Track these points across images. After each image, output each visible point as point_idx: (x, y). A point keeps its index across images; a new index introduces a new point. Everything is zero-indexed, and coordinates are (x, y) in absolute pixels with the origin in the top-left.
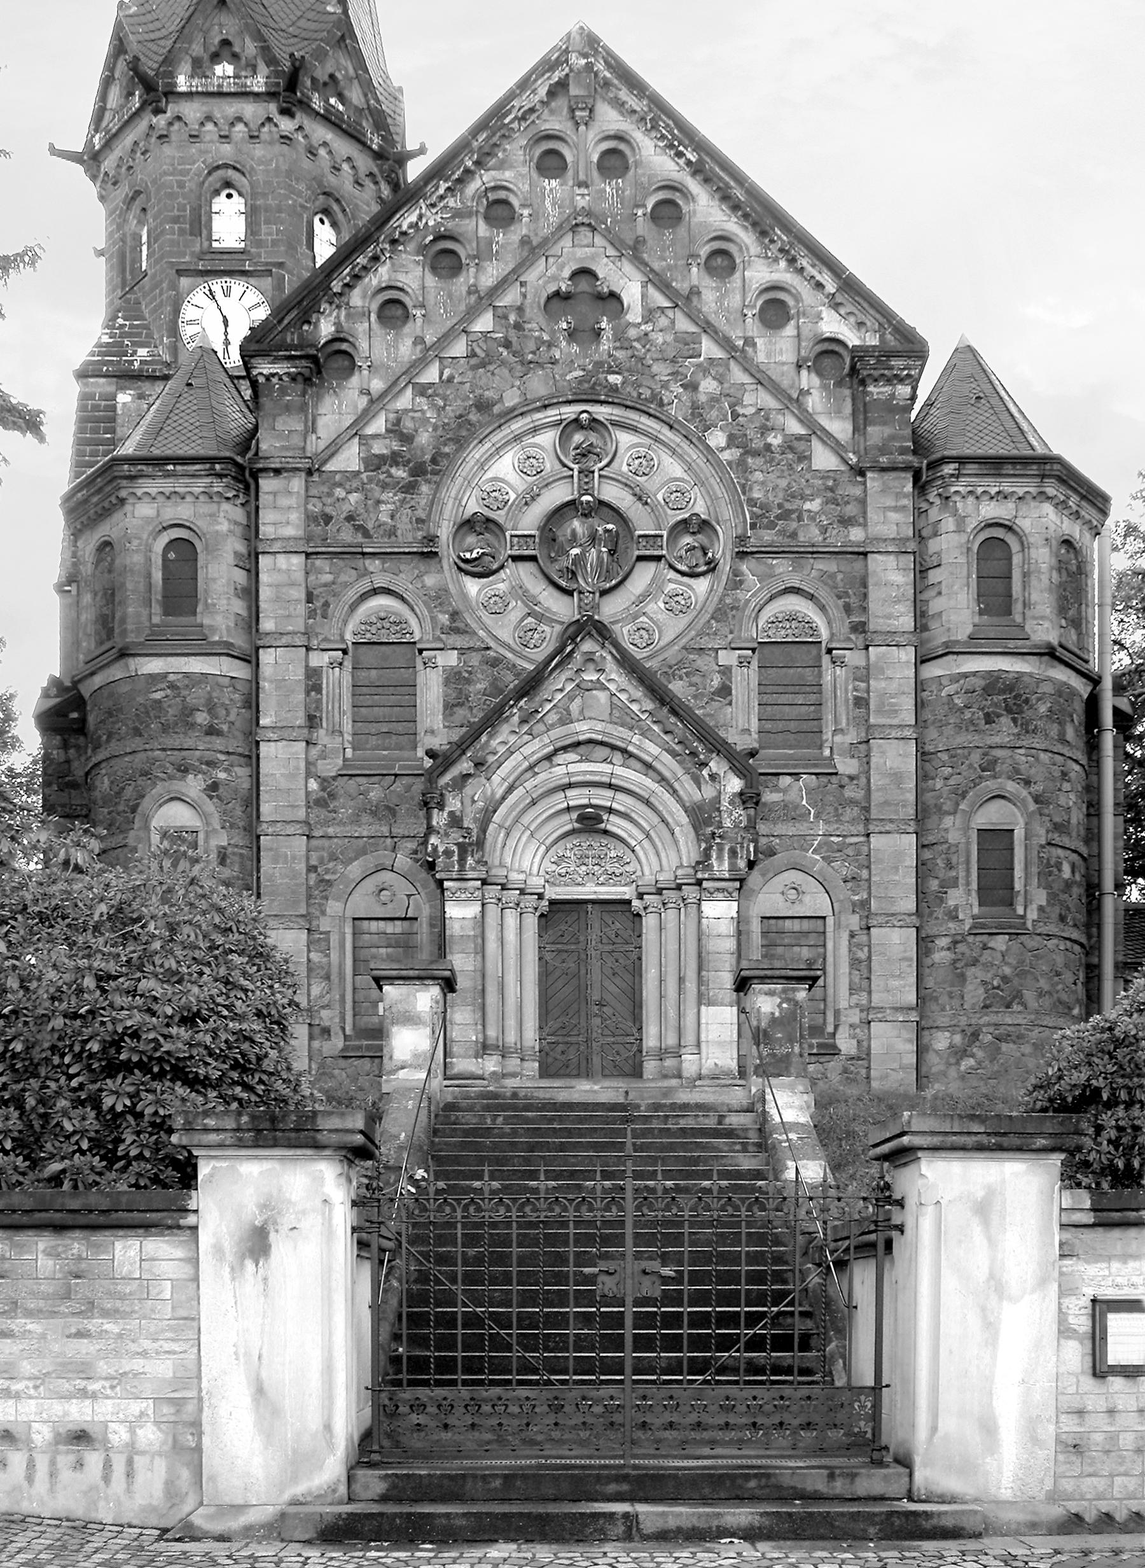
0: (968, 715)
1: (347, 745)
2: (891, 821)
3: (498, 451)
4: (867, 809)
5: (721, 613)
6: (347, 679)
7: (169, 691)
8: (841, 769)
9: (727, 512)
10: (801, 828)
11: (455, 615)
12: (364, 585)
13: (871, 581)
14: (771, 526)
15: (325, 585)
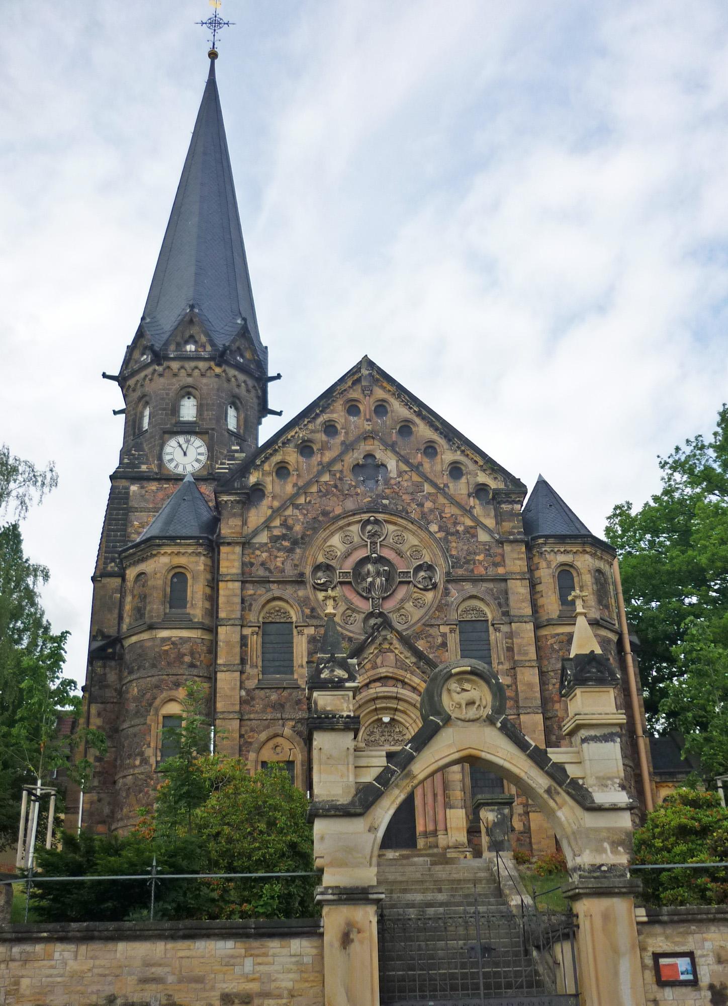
2: (530, 707)
3: (332, 534)
4: (517, 701)
5: (440, 608)
6: (260, 640)
7: (172, 646)
9: (441, 561)
11: (313, 610)
12: (269, 595)
13: (510, 592)
14: (461, 567)
15: (251, 595)
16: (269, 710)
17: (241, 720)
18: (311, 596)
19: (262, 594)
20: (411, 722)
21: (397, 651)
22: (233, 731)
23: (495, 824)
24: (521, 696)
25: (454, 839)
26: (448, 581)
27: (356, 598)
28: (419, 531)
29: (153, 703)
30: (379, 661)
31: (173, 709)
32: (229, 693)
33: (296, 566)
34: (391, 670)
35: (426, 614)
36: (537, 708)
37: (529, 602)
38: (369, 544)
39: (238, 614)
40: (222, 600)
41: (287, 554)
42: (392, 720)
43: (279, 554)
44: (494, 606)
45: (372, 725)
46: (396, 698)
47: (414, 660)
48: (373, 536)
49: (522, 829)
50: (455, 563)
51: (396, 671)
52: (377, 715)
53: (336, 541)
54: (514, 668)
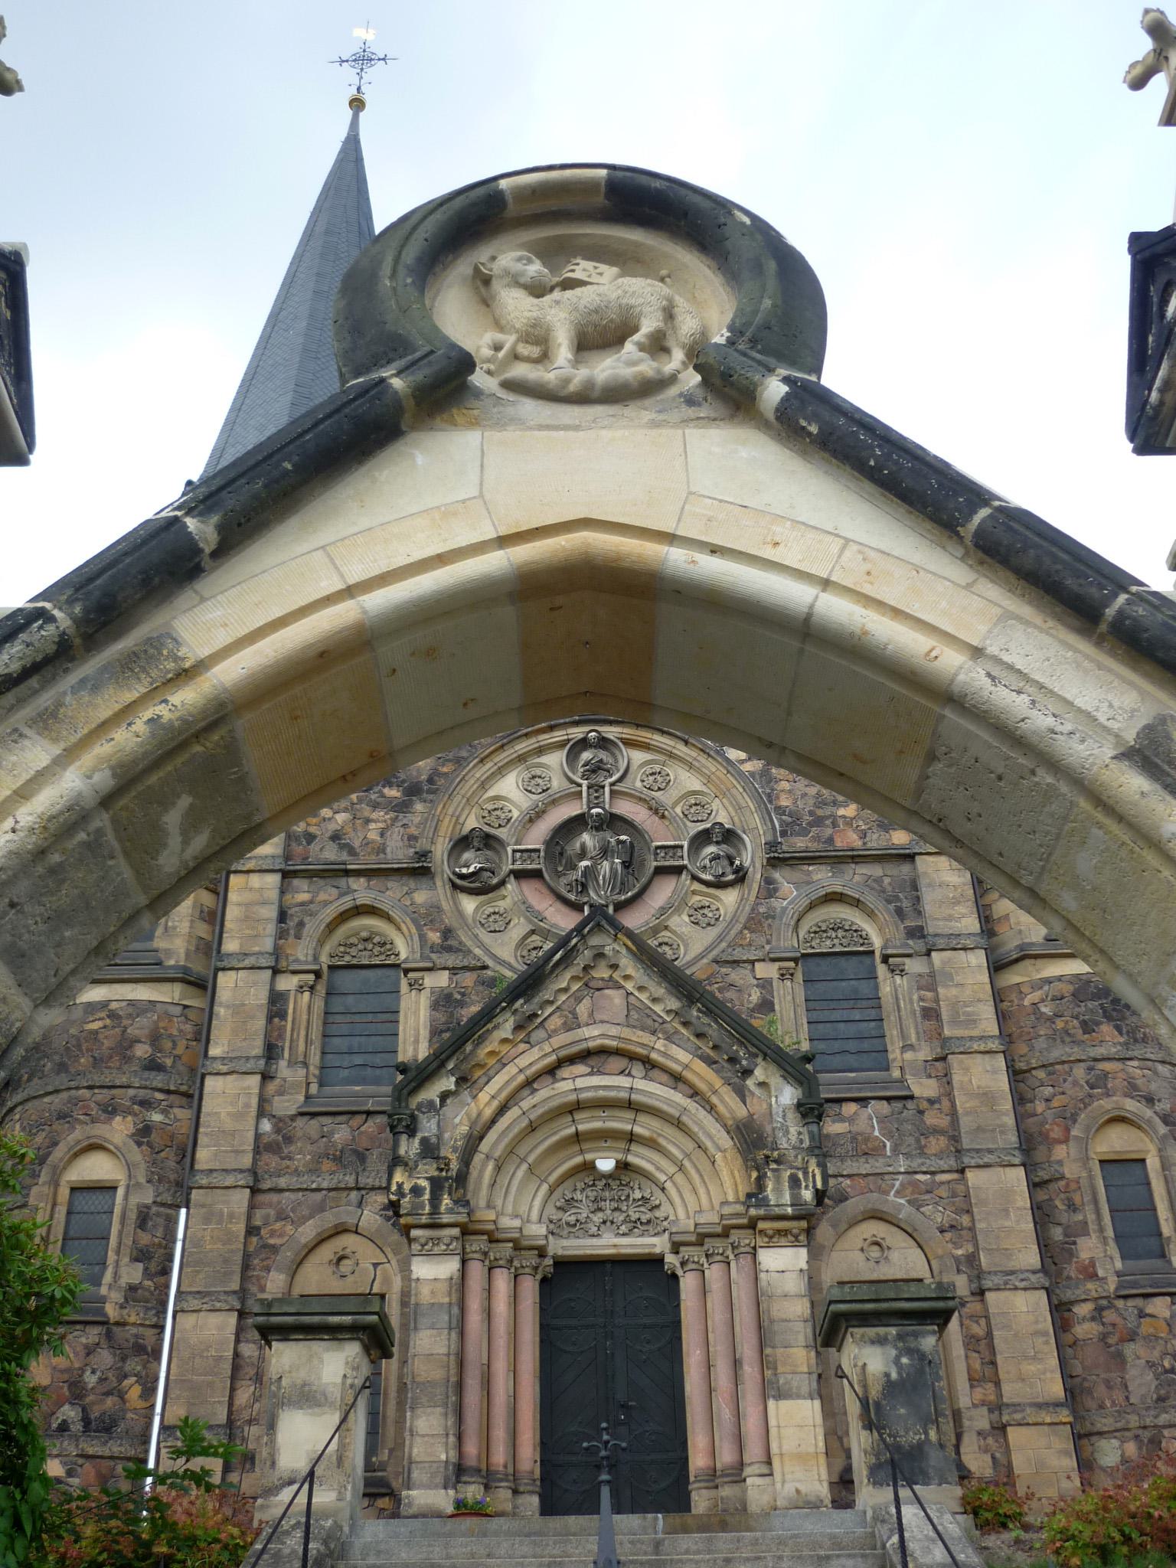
0: (1060, 1024)
1: (312, 1079)
2: (990, 1151)
3: (500, 772)
4: (955, 1139)
5: (755, 922)
6: (319, 1004)
7: (108, 1021)
8: (916, 1091)
9: (756, 821)
10: (877, 1165)
11: (447, 933)
12: (346, 903)
13: (923, 883)
14: (804, 832)
15: (302, 904)
16: (327, 1165)
17: (255, 1191)
18: (445, 905)
19: (330, 899)
20: (672, 1169)
21: (629, 986)
22: (231, 1216)
23: (891, 1387)
24: (966, 1123)
25: (789, 1489)
26: (774, 862)
27: (552, 909)
28: (702, 758)
29: (49, 1154)
30: (583, 1009)
31: (97, 1168)
32: (229, 1124)
33: (412, 838)
34: (614, 1031)
35: (720, 938)
36: (1007, 1151)
37: (971, 904)
38: (585, 788)
39: (268, 944)
40: (232, 913)
41: (392, 815)
42: (623, 1166)
43: (374, 816)
44: (885, 913)
45: (569, 1184)
46: (630, 1105)
47: (674, 1004)
48: (594, 771)
49: (989, 1473)
50: (787, 824)
51: (627, 1033)
52: (582, 1152)
53: (510, 788)
54: (944, 1059)
